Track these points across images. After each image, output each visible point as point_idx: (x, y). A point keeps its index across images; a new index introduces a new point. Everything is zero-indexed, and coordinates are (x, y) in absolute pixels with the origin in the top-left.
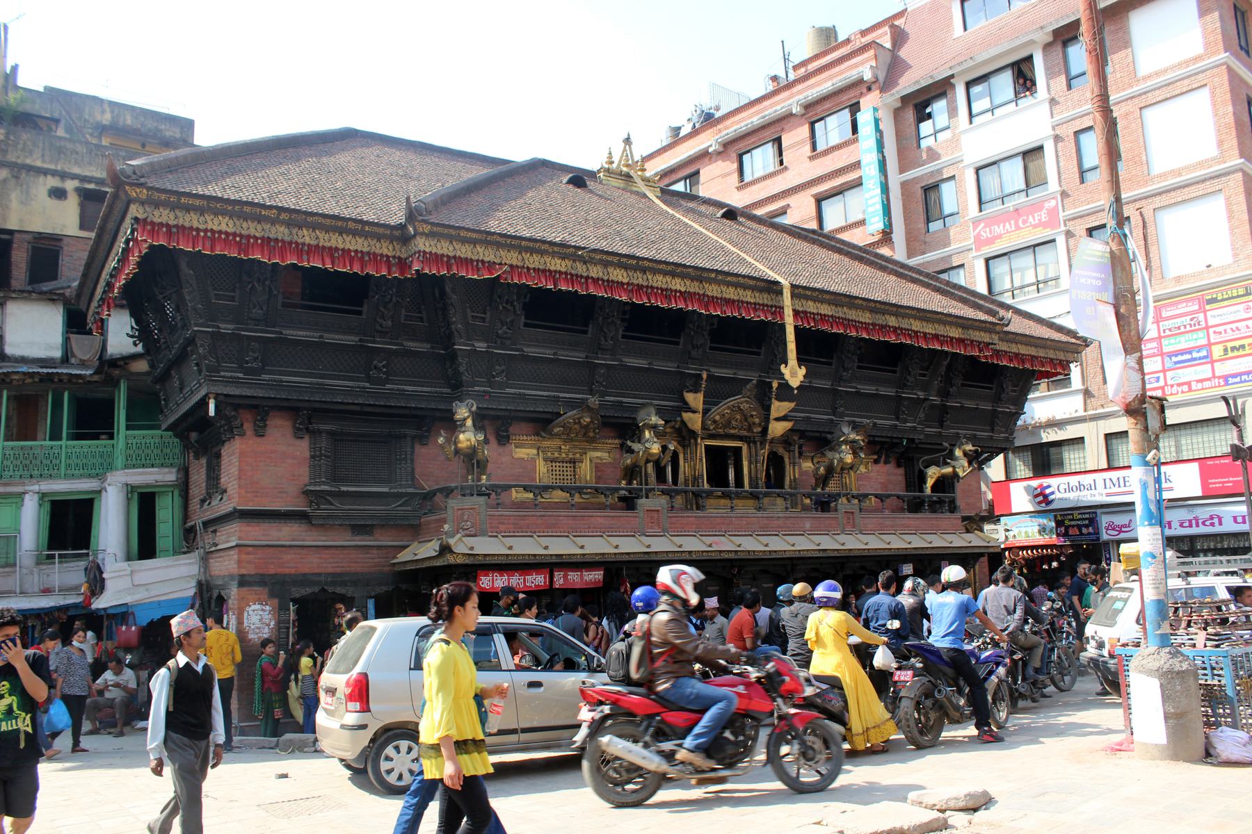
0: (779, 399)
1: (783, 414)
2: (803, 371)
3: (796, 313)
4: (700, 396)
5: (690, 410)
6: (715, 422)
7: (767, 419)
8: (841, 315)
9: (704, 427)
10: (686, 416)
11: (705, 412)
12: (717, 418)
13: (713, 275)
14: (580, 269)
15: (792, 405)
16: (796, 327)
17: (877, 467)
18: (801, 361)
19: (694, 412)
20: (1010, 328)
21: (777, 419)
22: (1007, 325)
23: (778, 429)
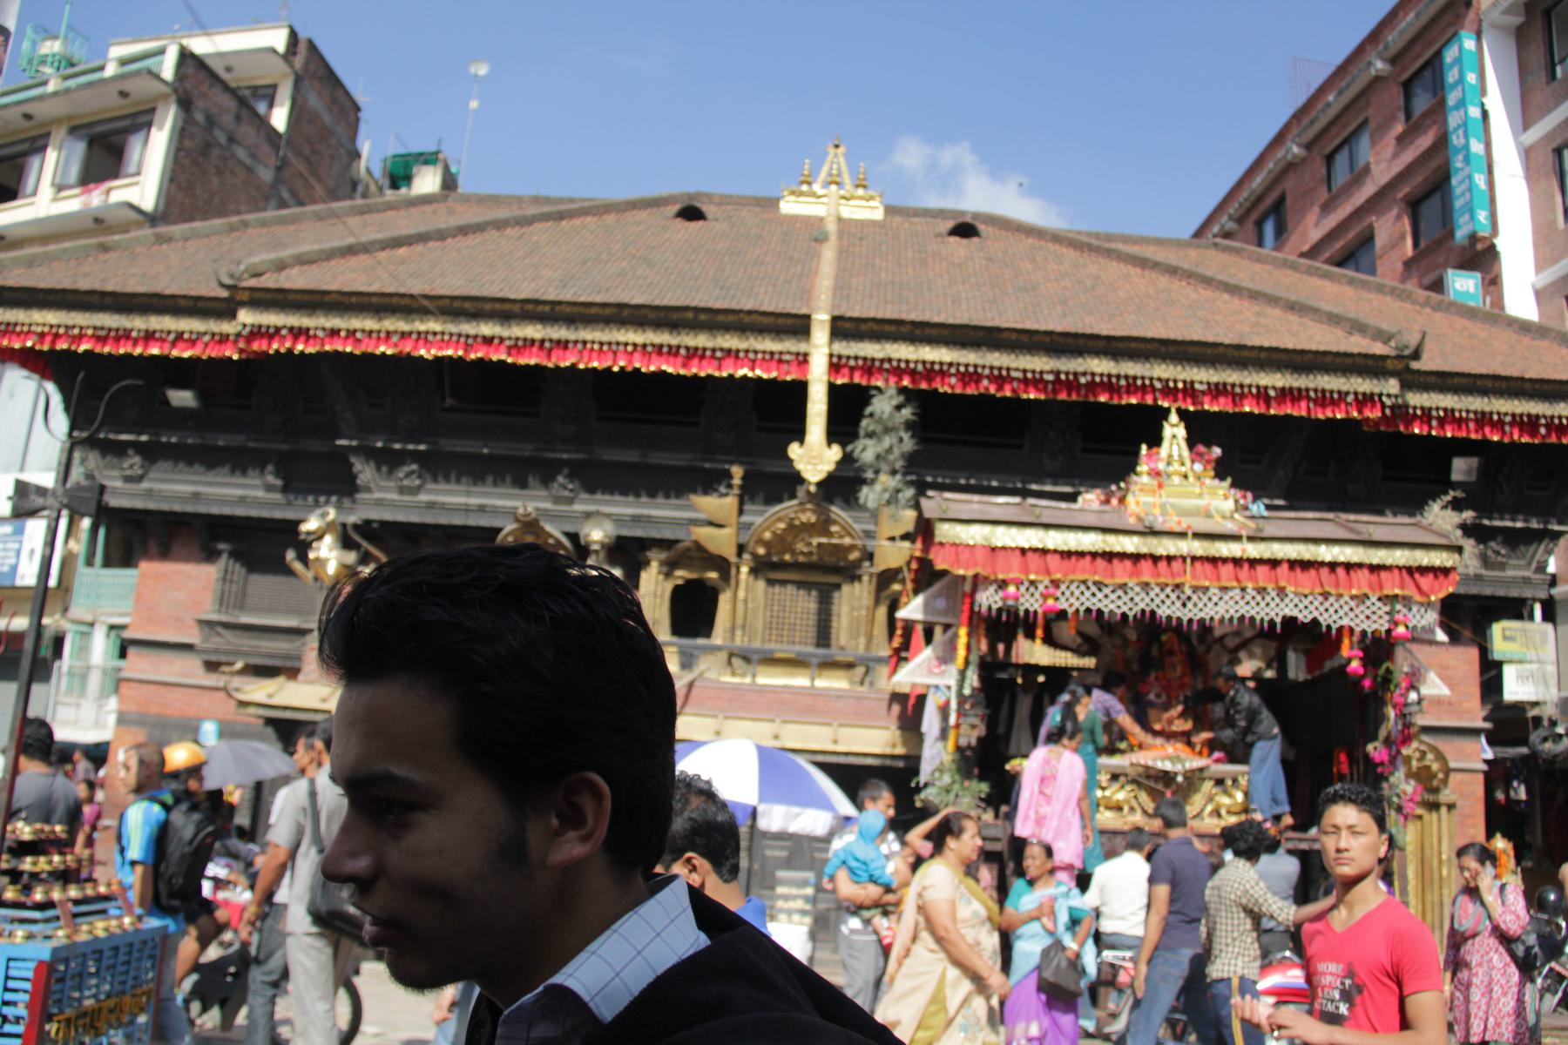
4: (730, 502)
6: (767, 544)
9: (741, 549)
12: (767, 535)
18: (830, 441)
20: (1425, 364)
22: (1416, 355)
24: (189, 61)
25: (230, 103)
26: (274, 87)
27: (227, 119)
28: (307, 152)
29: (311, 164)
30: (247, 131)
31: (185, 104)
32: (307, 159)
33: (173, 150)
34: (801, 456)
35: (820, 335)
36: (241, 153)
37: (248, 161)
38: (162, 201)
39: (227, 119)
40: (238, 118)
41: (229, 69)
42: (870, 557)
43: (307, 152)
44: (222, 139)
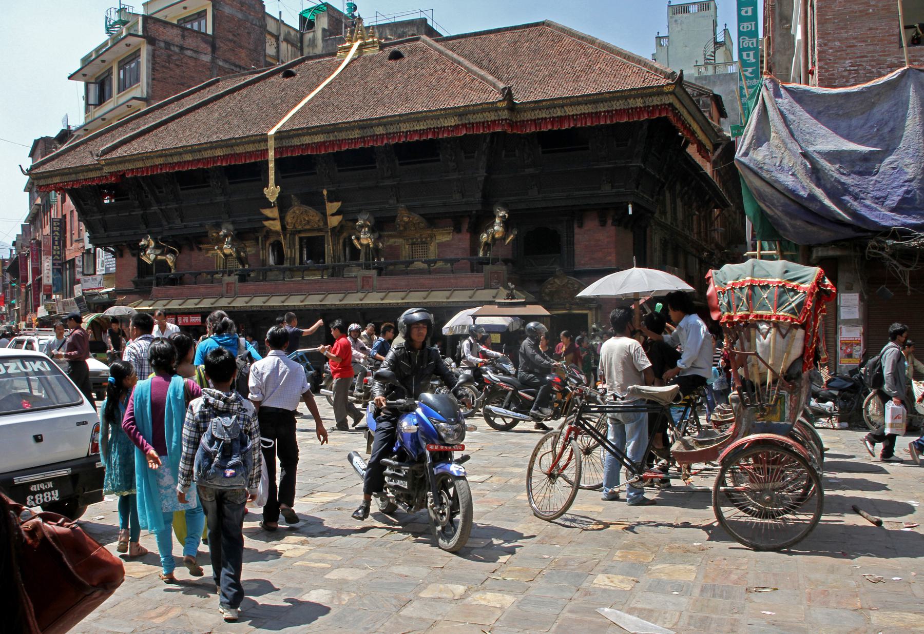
0: (331, 201)
1: (335, 211)
2: (278, 189)
3: (276, 150)
5: (268, 219)
7: (324, 215)
8: (332, 138)
9: (284, 227)
10: (266, 223)
11: (282, 219)
13: (234, 141)
14: (170, 160)
15: (339, 204)
16: (278, 162)
17: (460, 236)
18: (276, 184)
19: (274, 219)
21: (333, 215)
23: (334, 221)
24: (150, 21)
25: (176, 31)
26: (205, 11)
27: (178, 40)
28: (231, 37)
29: (235, 42)
30: (190, 42)
31: (151, 41)
32: (231, 41)
33: (150, 66)
34: (268, 192)
35: (271, 144)
36: (189, 53)
37: (194, 55)
38: (150, 91)
39: (178, 40)
40: (183, 37)
41: (185, 8)
42: (326, 223)
43: (231, 37)
44: (177, 50)
